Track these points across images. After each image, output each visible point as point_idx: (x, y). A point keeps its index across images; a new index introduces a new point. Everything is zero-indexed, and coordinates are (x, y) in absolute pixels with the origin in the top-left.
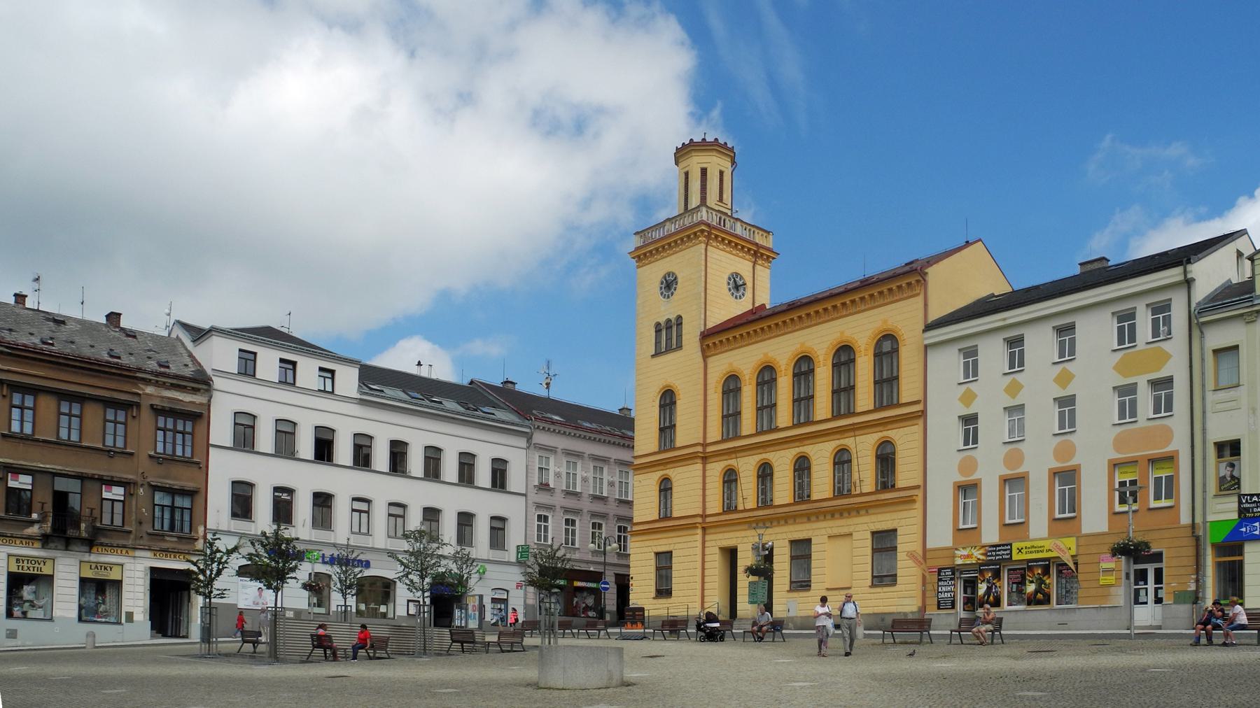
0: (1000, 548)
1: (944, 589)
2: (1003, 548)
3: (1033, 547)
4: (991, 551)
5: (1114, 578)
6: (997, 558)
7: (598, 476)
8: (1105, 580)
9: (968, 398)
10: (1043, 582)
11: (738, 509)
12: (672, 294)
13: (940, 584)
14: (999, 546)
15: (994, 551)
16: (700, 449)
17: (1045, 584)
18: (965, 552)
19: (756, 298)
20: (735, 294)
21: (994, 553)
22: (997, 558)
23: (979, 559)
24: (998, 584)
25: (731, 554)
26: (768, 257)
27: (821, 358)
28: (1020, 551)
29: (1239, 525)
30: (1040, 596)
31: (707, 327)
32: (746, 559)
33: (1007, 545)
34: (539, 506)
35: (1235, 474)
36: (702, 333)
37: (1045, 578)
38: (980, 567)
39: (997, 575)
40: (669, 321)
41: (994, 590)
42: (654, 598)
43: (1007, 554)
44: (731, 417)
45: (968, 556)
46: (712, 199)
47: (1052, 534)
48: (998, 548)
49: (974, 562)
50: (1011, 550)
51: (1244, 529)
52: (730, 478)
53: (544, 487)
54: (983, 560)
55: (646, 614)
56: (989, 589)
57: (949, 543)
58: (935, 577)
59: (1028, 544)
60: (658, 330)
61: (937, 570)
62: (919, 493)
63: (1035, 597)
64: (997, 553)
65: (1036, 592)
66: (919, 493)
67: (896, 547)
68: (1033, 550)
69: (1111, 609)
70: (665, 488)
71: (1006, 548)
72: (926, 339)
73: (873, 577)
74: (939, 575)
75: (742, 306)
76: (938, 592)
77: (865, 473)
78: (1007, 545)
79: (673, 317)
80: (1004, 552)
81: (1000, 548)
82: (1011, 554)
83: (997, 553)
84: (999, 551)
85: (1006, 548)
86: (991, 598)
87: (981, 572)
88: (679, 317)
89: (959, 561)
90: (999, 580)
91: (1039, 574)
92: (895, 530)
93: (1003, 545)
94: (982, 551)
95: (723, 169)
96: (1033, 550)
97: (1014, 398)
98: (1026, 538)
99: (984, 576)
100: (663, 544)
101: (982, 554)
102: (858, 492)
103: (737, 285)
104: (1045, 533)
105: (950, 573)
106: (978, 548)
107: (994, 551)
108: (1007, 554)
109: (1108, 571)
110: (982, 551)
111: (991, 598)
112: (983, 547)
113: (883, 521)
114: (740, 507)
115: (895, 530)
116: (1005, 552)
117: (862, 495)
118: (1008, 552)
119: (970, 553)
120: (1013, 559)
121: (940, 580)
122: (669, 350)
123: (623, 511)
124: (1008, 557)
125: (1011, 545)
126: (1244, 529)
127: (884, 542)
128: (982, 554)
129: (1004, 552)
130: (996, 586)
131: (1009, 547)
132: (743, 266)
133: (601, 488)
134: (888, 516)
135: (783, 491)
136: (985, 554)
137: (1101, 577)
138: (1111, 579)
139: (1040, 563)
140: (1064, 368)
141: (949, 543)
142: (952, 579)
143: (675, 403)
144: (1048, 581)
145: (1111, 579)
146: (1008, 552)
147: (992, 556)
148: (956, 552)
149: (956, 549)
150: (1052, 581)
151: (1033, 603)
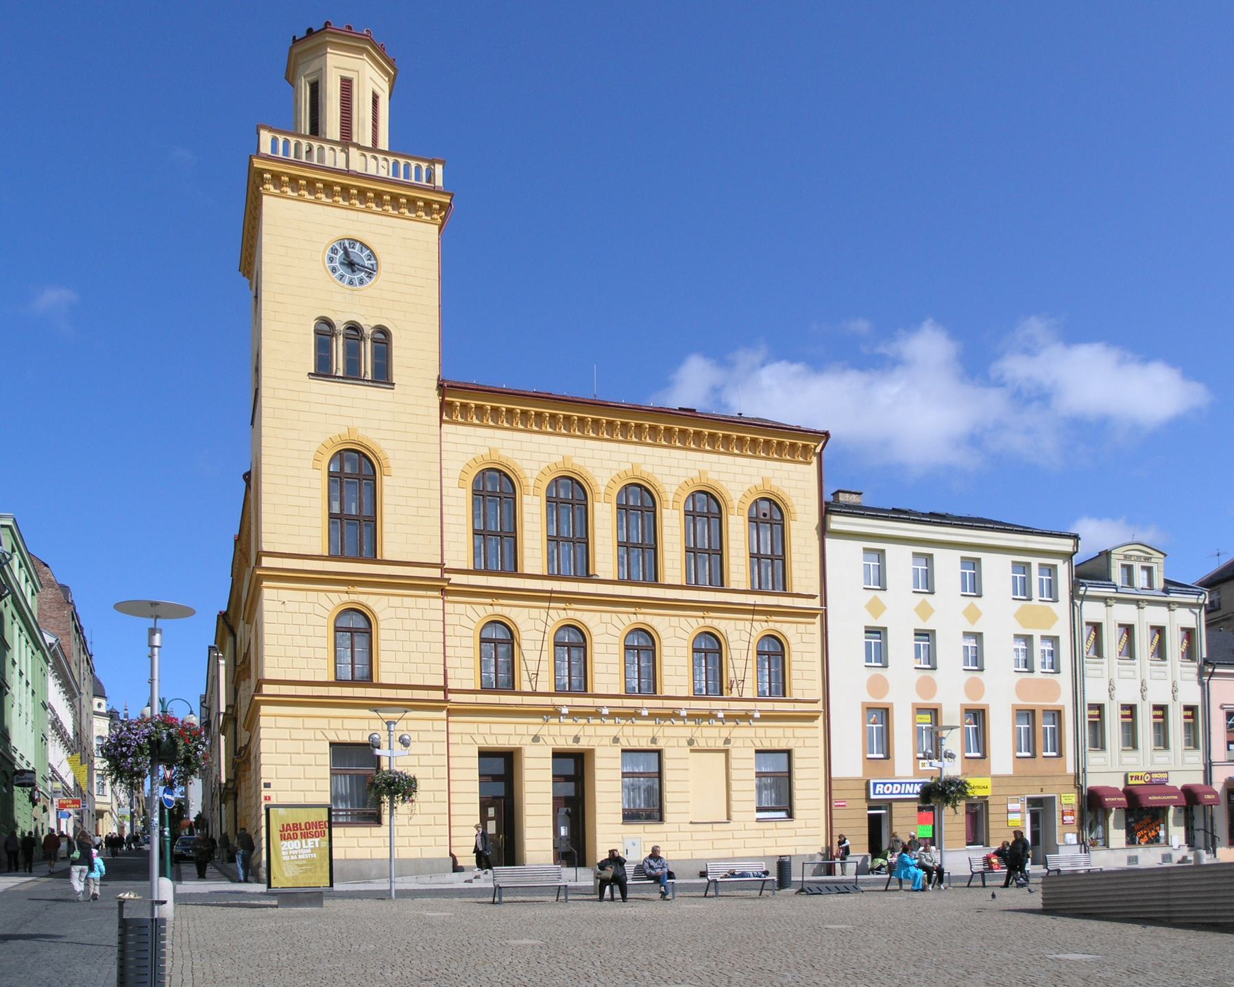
9: (875, 608)
97: (925, 621)
102: (735, 694)
113: (776, 736)
122: (353, 374)
140: (924, 600)
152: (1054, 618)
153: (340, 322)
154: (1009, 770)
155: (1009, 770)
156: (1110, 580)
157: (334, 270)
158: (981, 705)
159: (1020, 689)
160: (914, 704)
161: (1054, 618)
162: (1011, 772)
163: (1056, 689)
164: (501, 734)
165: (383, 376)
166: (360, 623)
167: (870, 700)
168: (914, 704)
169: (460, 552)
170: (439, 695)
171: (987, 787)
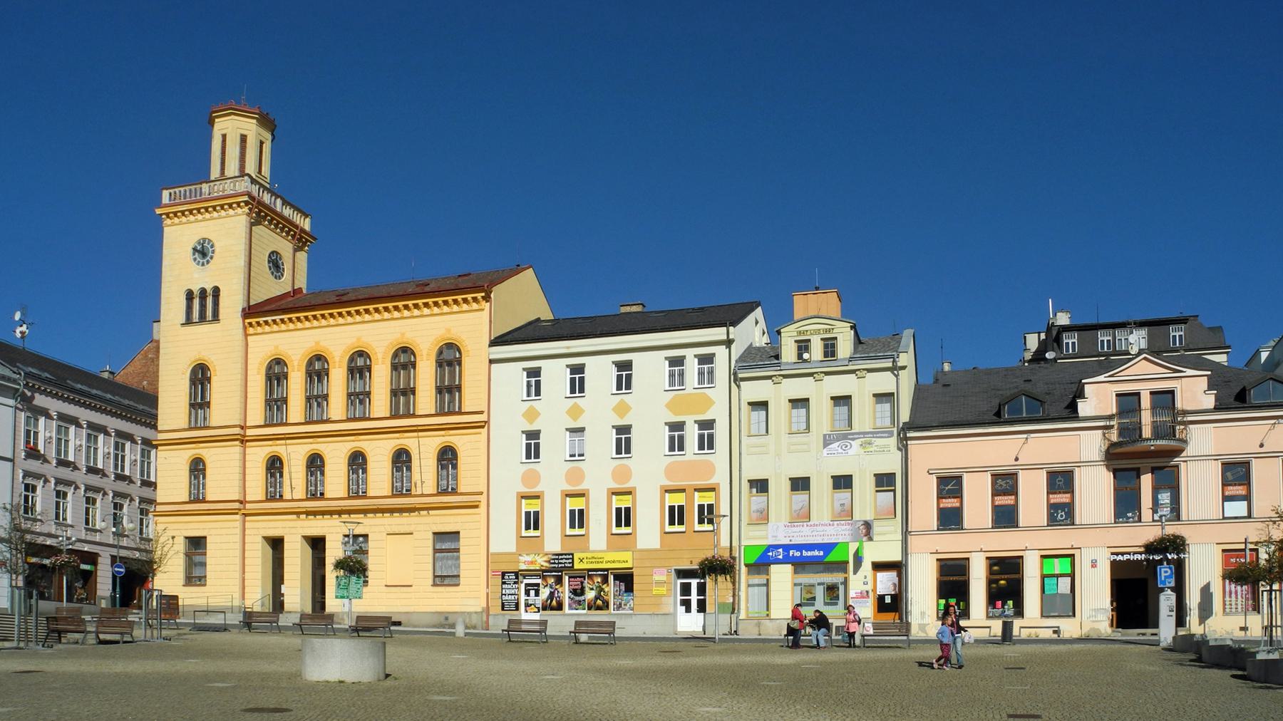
0: (562, 557)
1: (508, 592)
2: (566, 557)
3: (593, 558)
4: (554, 559)
5: (665, 589)
6: (560, 565)
7: (92, 445)
10: (602, 590)
11: (284, 498)
12: (208, 262)
13: (504, 586)
14: (562, 555)
15: (557, 559)
16: (237, 430)
17: (604, 592)
18: (529, 558)
19: (296, 281)
20: (275, 273)
21: (557, 561)
22: (560, 565)
23: (542, 566)
24: (560, 590)
25: (276, 544)
26: (307, 240)
27: (380, 356)
28: (581, 561)
30: (599, 602)
31: (252, 303)
32: (334, 552)
33: (569, 554)
34: (27, 474)
36: (244, 310)
37: (604, 587)
38: (542, 574)
39: (559, 580)
40: (203, 292)
41: (556, 595)
42: (184, 586)
43: (570, 563)
44: (275, 403)
45: (532, 563)
46: (251, 168)
47: (611, 547)
48: (560, 557)
49: (538, 568)
50: (573, 559)
52: (275, 466)
53: (33, 453)
54: (546, 567)
55: (180, 603)
56: (552, 594)
57: (513, 549)
58: (499, 580)
59: (589, 555)
60: (190, 296)
61: (500, 573)
62: (483, 498)
63: (595, 603)
64: (560, 561)
65: (597, 598)
66: (483, 498)
67: (459, 549)
68: (593, 560)
69: (663, 616)
70: (197, 468)
71: (568, 557)
72: (493, 353)
73: (435, 577)
74: (503, 578)
75: (281, 287)
76: (502, 595)
77: (425, 473)
78: (569, 554)
79: (209, 287)
80: (566, 561)
81: (562, 557)
82: (573, 563)
83: (560, 561)
84: (562, 559)
85: (568, 557)
87: (544, 578)
88: (216, 291)
89: (523, 567)
90: (562, 586)
91: (598, 582)
92: (458, 533)
93: (566, 555)
95: (263, 140)
96: (593, 560)
98: (586, 549)
99: (547, 582)
100: (195, 527)
101: (546, 561)
103: (275, 263)
104: (604, 547)
105: (514, 577)
106: (541, 555)
107: (557, 559)
108: (570, 563)
109: (659, 583)
110: (546, 558)
112: (547, 554)
113: (446, 522)
114: (287, 496)
115: (458, 533)
116: (568, 561)
117: (422, 495)
118: (570, 561)
120: (575, 567)
121: (504, 583)
122: (203, 318)
123: (146, 493)
124: (571, 565)
125: (572, 554)
127: (446, 542)
128: (546, 561)
129: (566, 561)
130: (558, 592)
131: (571, 557)
132: (285, 247)
133: (95, 459)
134: (452, 519)
135: (336, 481)
136: (549, 562)
137: (654, 588)
138: (663, 590)
139: (599, 573)
141: (513, 549)
142: (515, 583)
143: (209, 380)
144: (606, 590)
145: (663, 590)
146: (570, 561)
147: (554, 563)
148: (520, 558)
149: (520, 555)
150: (611, 588)
151: (593, 608)
152: (709, 403)
153: (196, 289)
154: (656, 544)
155: (656, 544)
157: (212, 258)
158: (535, 492)
159: (669, 471)
160: (562, 491)
161: (709, 403)
162: (658, 546)
163: (711, 469)
164: (275, 527)
168: (562, 491)
170: (237, 505)
171: (627, 561)
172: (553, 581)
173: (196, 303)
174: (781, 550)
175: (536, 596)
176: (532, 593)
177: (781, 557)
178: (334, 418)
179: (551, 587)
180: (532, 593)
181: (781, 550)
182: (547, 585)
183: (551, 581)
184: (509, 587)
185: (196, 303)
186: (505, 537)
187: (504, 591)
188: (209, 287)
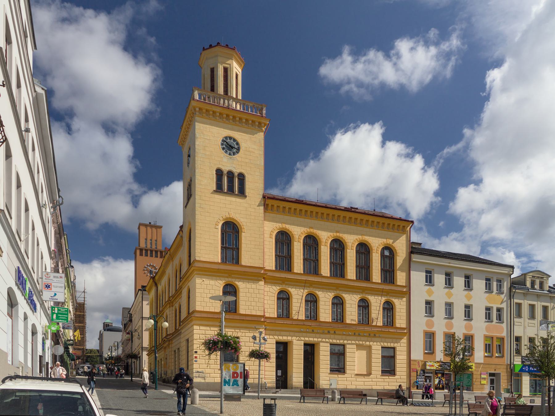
5: (486, 381)
8: (483, 382)
18: (431, 364)
29: (522, 367)
35: (518, 348)
51: (524, 368)
56: (440, 381)
71: (448, 364)
84: (445, 365)
85: (448, 364)
86: (441, 386)
87: (436, 374)
89: (428, 368)
94: (438, 364)
99: (438, 376)
110: (438, 364)
111: (441, 386)
117: (376, 326)
119: (433, 364)
126: (524, 368)
128: (438, 366)
155: (482, 361)
156: (526, 286)
165: (242, 193)
166: (231, 290)
167: (427, 329)
169: (270, 263)
172: (440, 375)
173: (225, 180)
174: (527, 367)
175: (429, 382)
176: (428, 380)
177: (527, 370)
178: (324, 275)
179: (439, 378)
180: (428, 380)
181: (527, 367)
182: (437, 378)
183: (440, 375)
184: (420, 377)
185: (225, 180)
186: (418, 354)
187: (418, 379)
188: (236, 171)
